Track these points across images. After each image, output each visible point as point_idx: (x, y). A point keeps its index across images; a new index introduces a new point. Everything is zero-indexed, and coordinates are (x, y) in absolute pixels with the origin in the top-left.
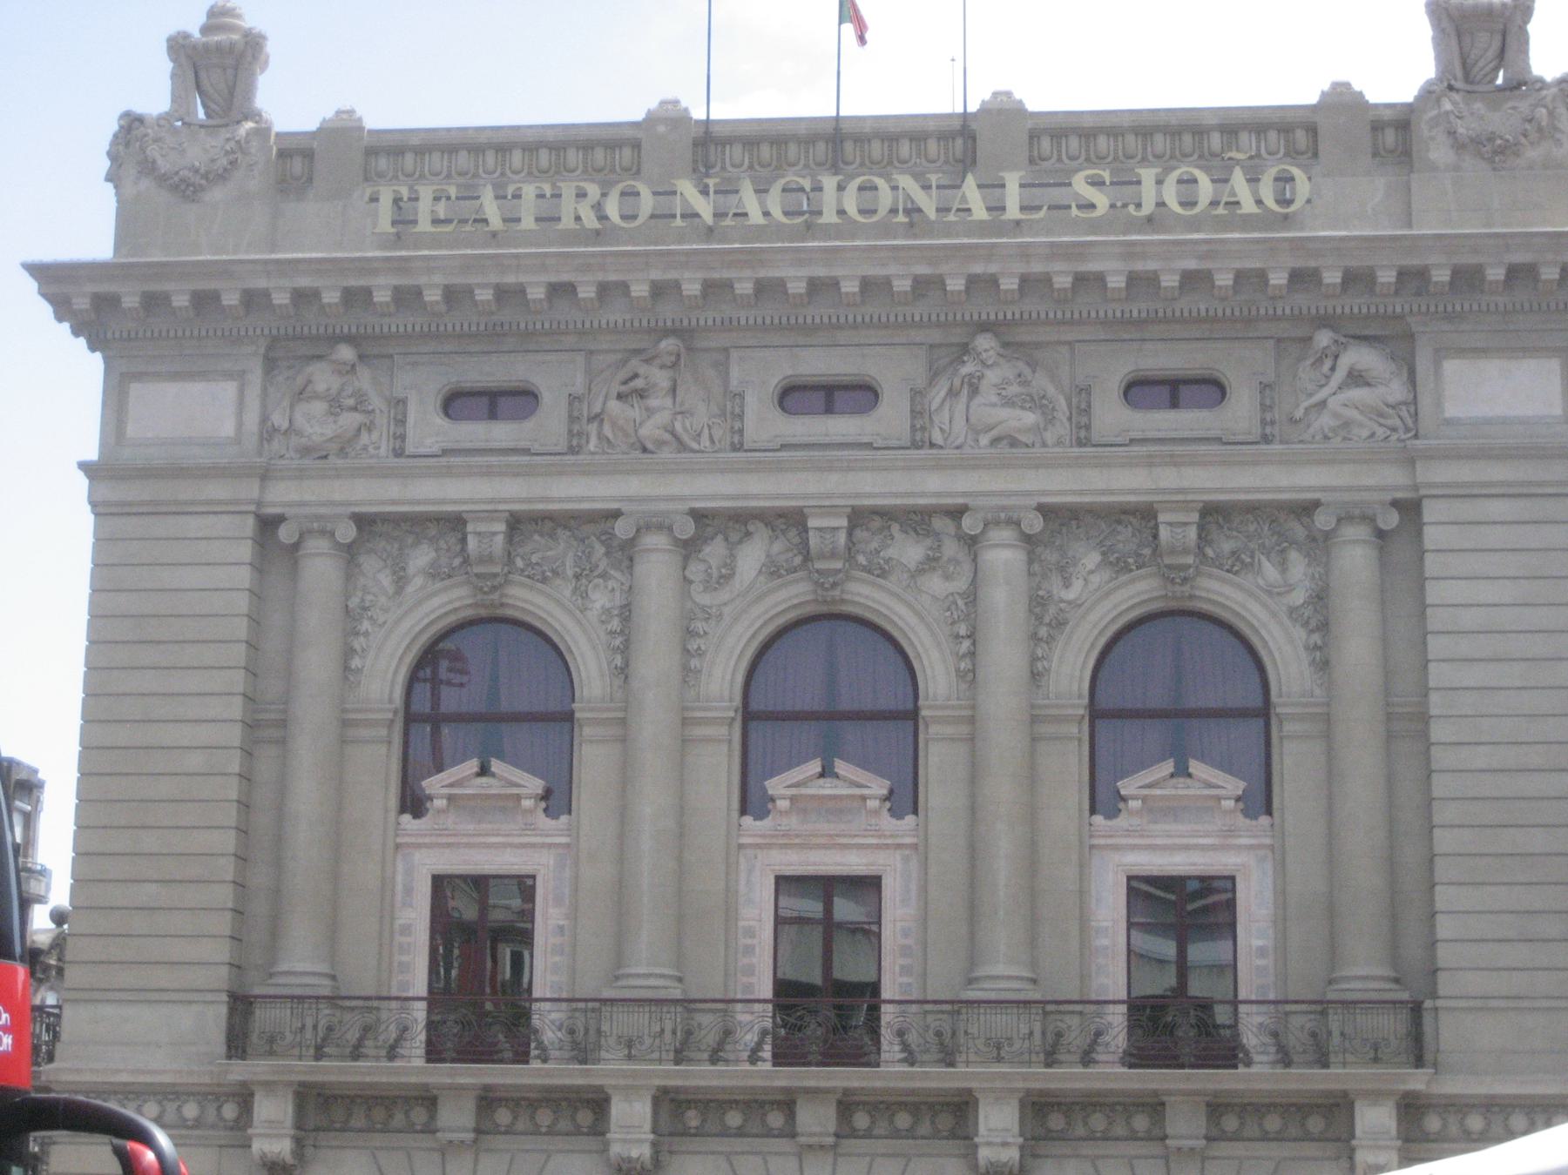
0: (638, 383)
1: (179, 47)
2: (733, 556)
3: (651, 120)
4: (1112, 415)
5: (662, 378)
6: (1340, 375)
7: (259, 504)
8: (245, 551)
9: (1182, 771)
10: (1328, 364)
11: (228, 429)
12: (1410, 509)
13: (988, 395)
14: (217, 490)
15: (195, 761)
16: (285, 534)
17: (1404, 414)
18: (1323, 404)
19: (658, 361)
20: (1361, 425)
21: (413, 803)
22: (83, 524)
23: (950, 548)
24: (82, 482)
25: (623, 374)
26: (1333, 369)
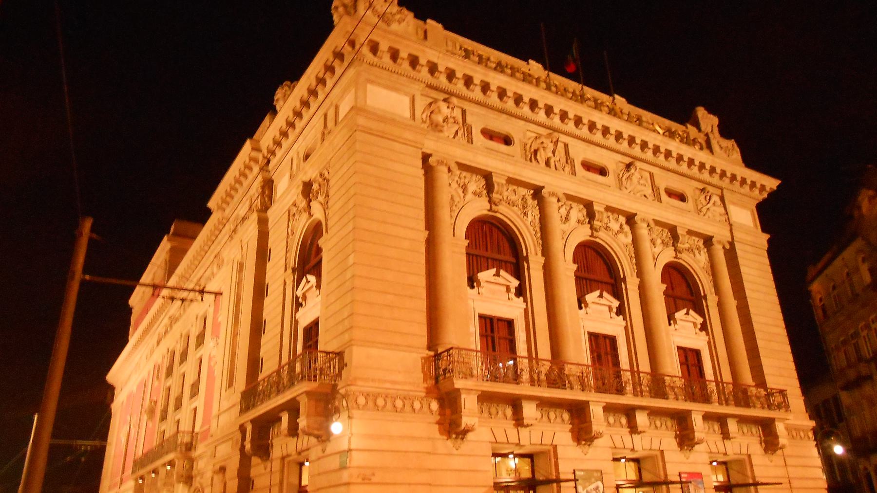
2: (568, 212)
4: (664, 196)
9: (687, 313)
11: (407, 114)
14: (408, 135)
18: (708, 209)
21: (472, 281)
23: (627, 228)
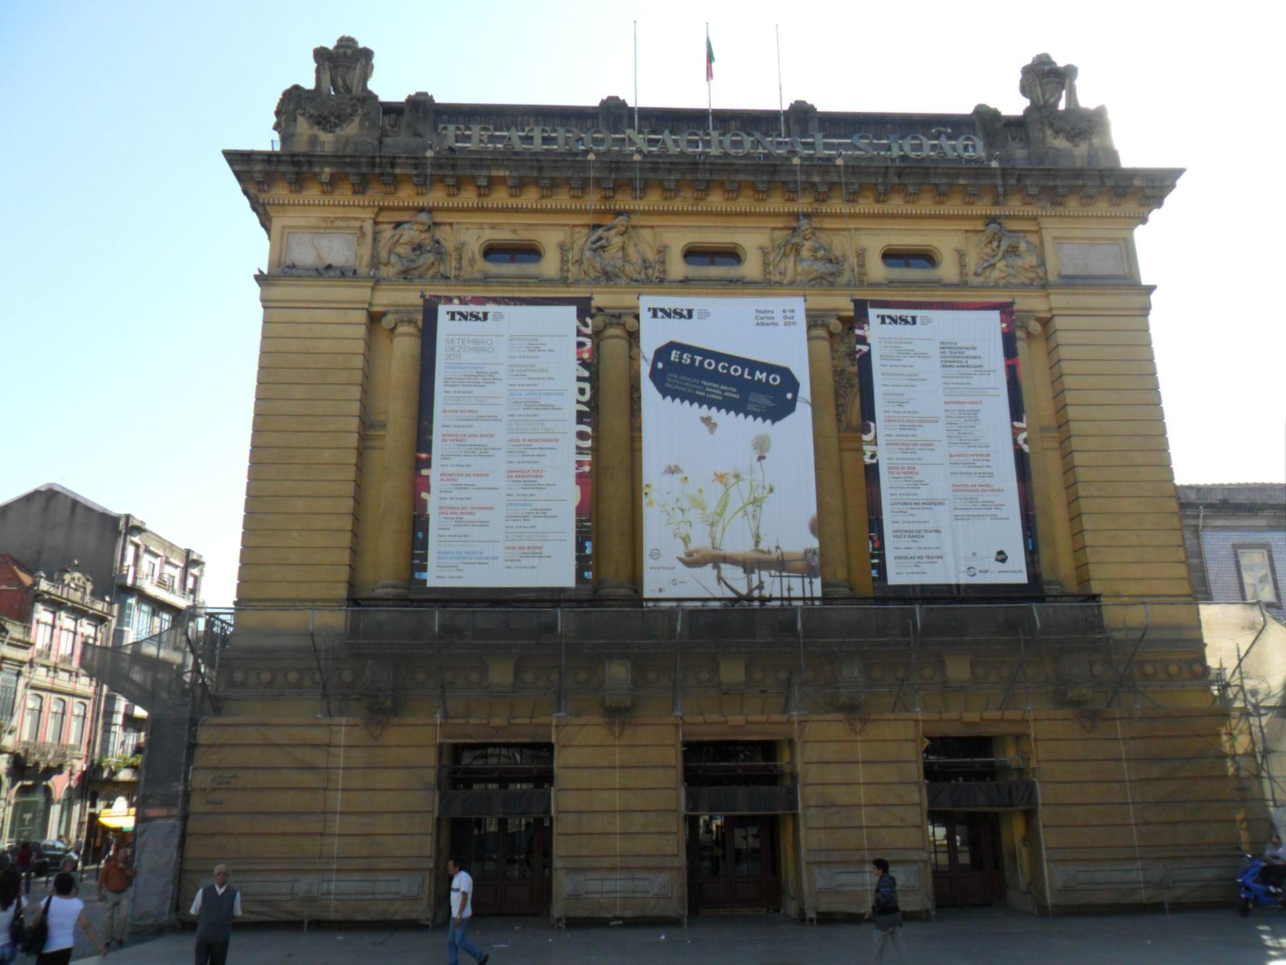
0: (603, 242)
1: (321, 55)
3: (603, 103)
5: (616, 241)
6: (1003, 247)
7: (370, 304)
8: (361, 331)
10: (995, 244)
12: (1045, 323)
13: (805, 253)
15: (327, 456)
16: (388, 321)
17: (1039, 271)
19: (613, 232)
20: (1015, 277)
22: (259, 312)
24: (256, 289)
25: (594, 237)
26: (998, 247)
